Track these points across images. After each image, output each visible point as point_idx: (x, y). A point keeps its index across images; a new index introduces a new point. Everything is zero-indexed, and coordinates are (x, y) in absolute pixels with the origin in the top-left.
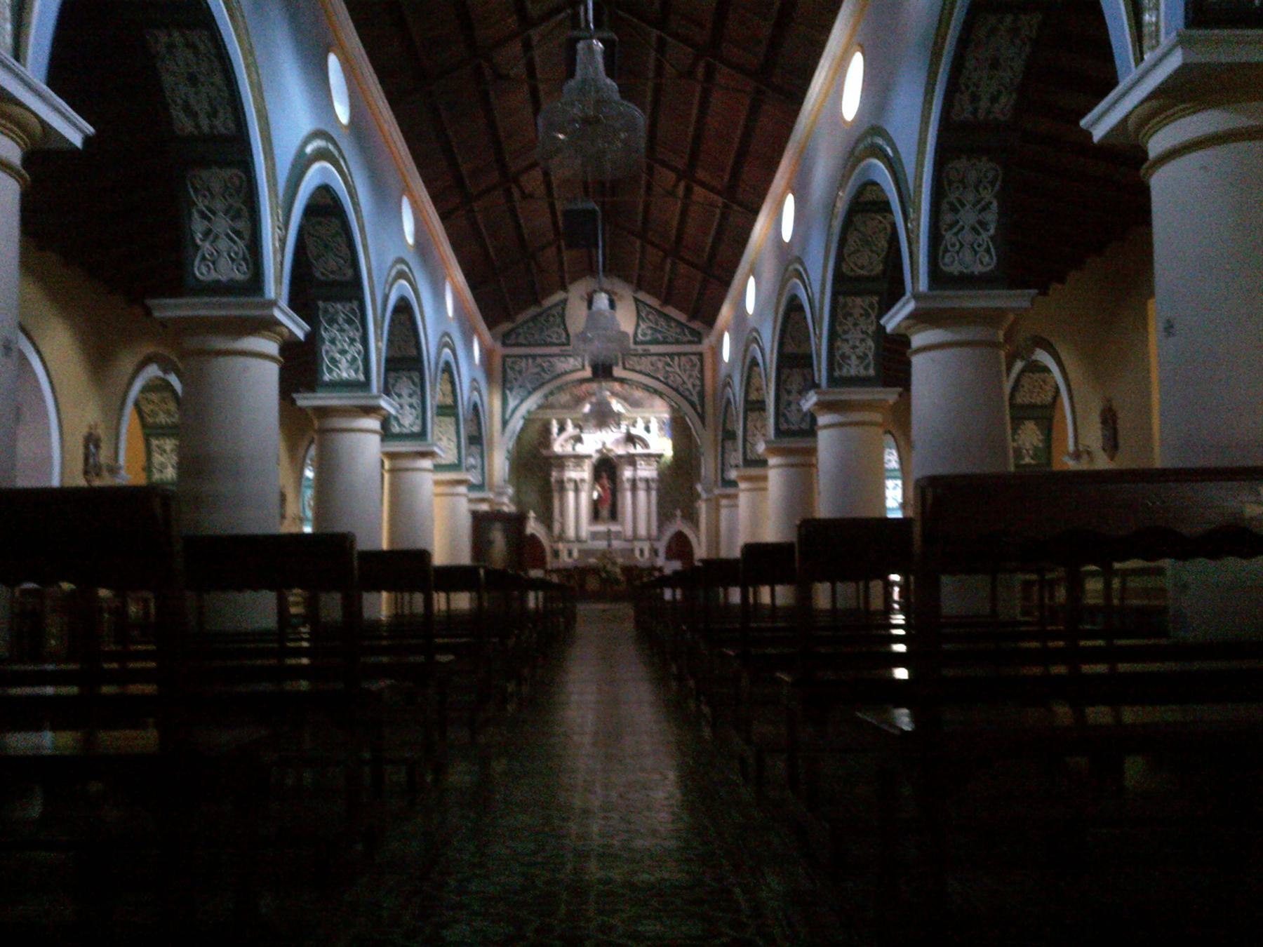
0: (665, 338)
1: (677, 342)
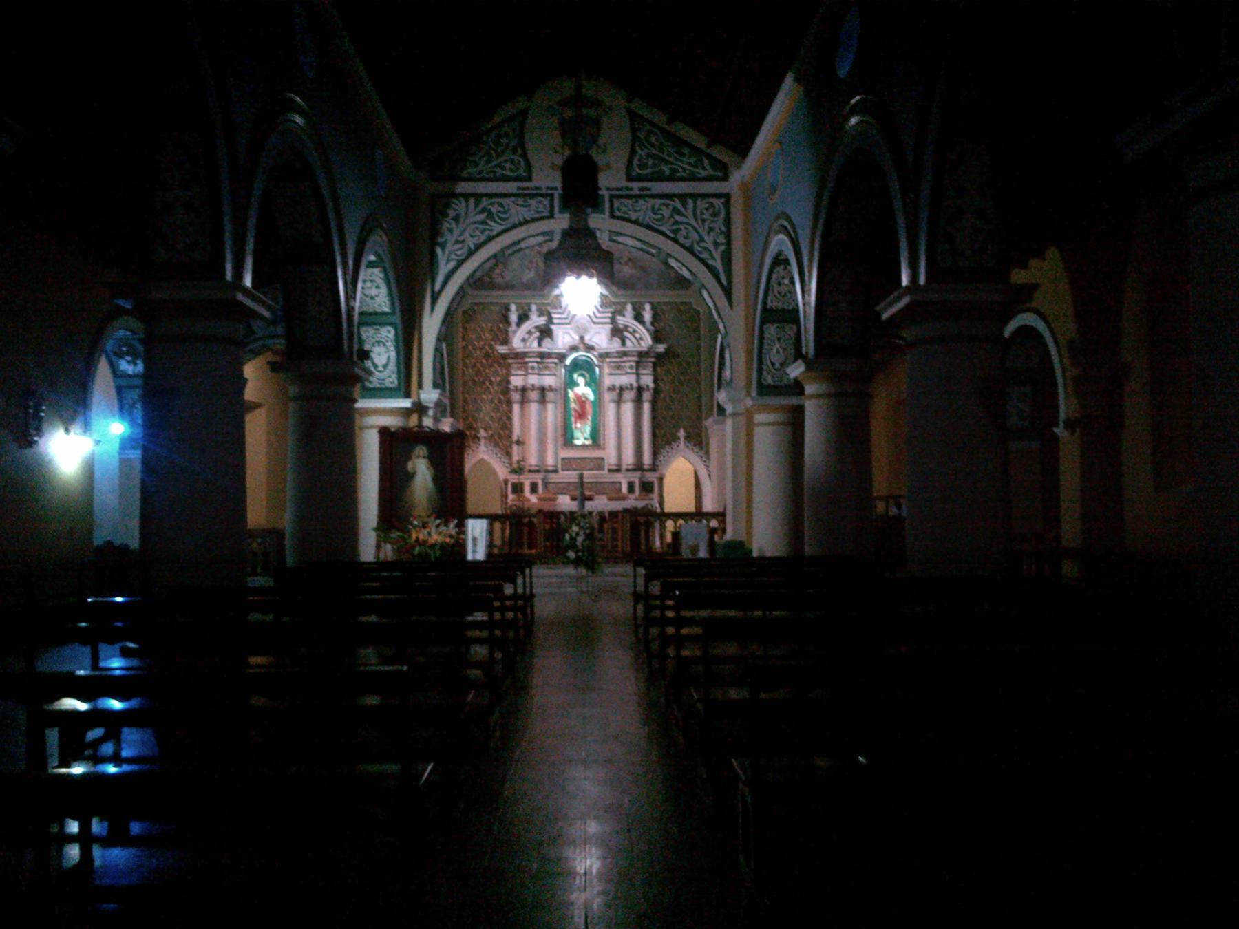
0: (674, 171)
1: (692, 178)
